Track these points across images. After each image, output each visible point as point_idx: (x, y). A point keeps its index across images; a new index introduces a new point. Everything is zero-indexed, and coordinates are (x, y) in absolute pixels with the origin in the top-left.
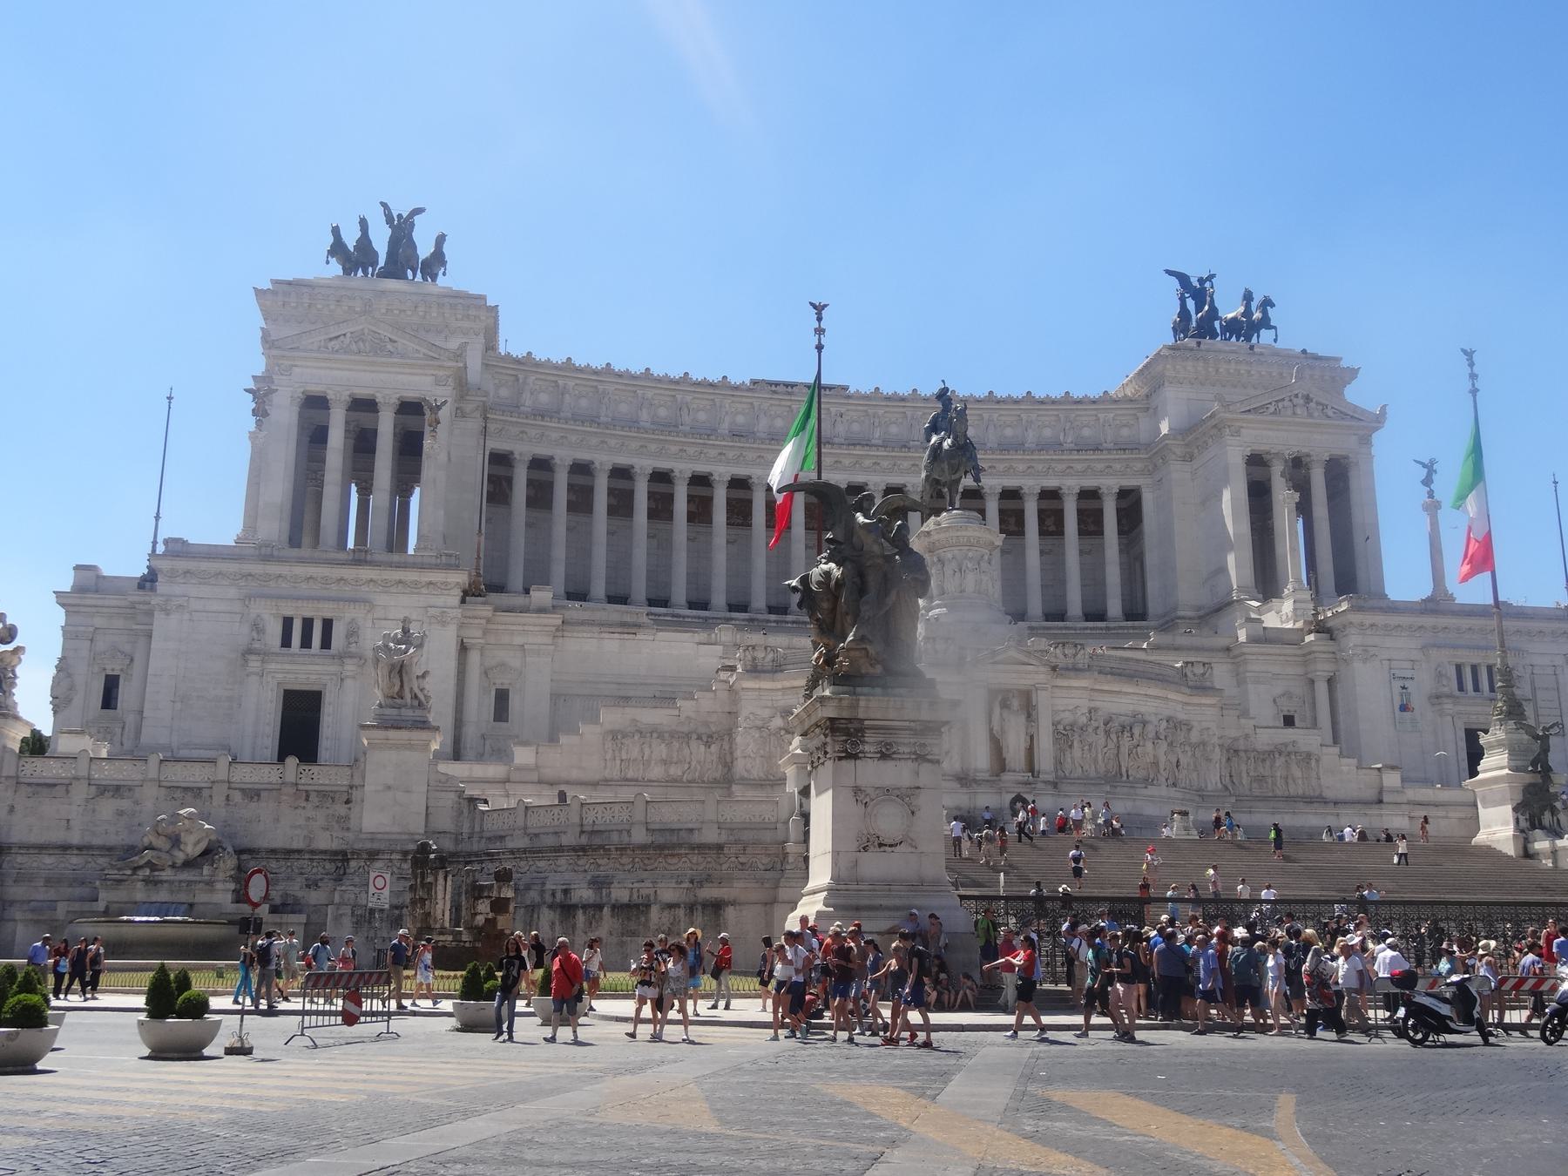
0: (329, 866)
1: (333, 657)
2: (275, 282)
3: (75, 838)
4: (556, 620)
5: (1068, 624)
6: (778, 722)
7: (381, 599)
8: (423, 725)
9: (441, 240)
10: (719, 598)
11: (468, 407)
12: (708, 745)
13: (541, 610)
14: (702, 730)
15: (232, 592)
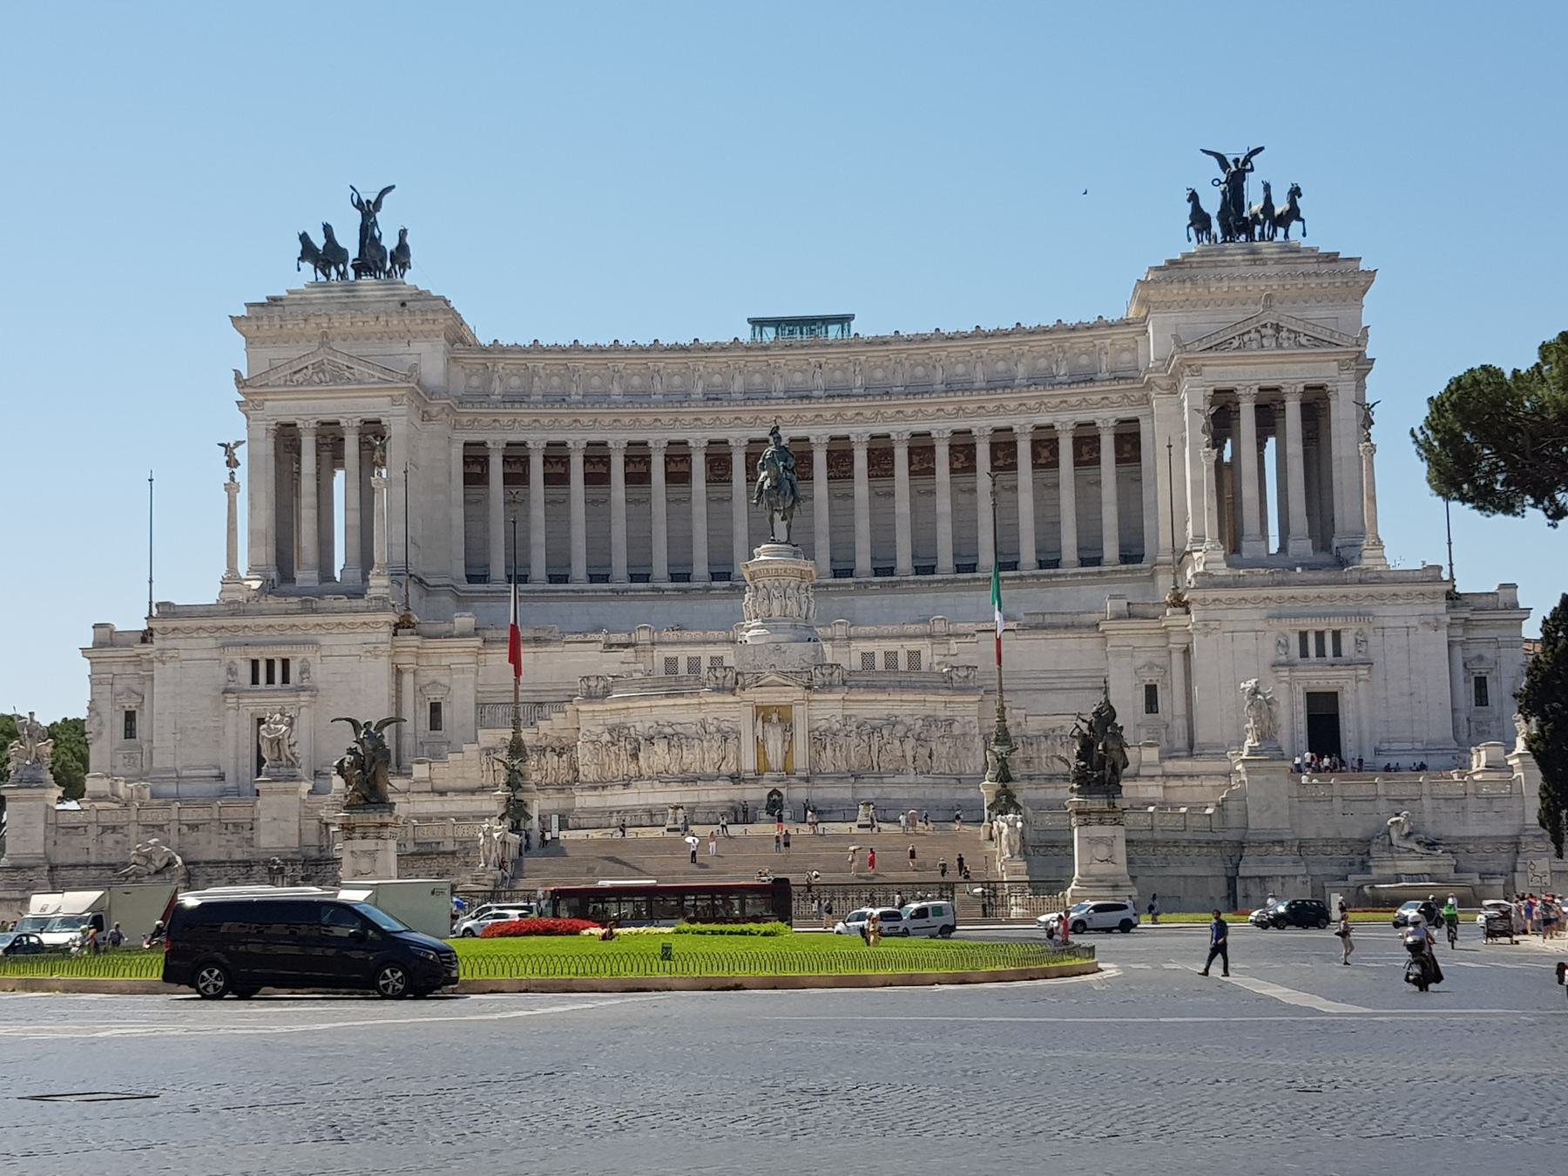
0: (243, 870)
1: (291, 690)
2: (248, 305)
3: (93, 860)
4: (477, 642)
5: (1059, 571)
6: (606, 737)
7: (326, 640)
8: (293, 778)
9: (403, 234)
10: (701, 569)
11: (434, 410)
12: (560, 755)
13: (463, 635)
14: (556, 744)
15: (211, 642)
